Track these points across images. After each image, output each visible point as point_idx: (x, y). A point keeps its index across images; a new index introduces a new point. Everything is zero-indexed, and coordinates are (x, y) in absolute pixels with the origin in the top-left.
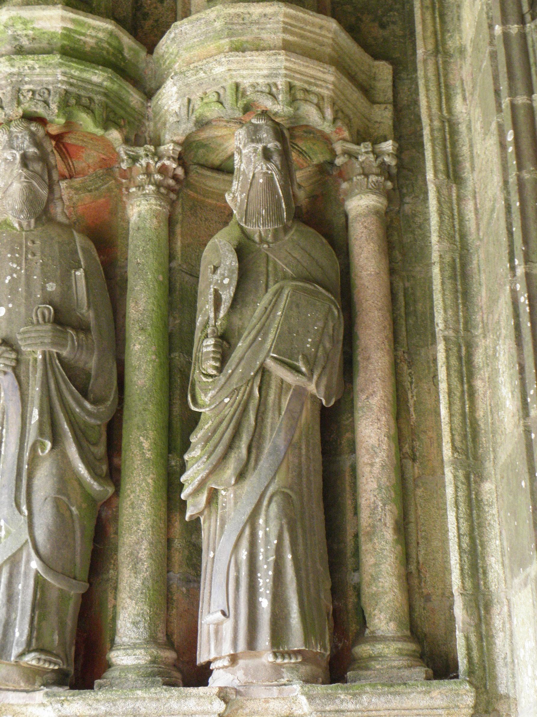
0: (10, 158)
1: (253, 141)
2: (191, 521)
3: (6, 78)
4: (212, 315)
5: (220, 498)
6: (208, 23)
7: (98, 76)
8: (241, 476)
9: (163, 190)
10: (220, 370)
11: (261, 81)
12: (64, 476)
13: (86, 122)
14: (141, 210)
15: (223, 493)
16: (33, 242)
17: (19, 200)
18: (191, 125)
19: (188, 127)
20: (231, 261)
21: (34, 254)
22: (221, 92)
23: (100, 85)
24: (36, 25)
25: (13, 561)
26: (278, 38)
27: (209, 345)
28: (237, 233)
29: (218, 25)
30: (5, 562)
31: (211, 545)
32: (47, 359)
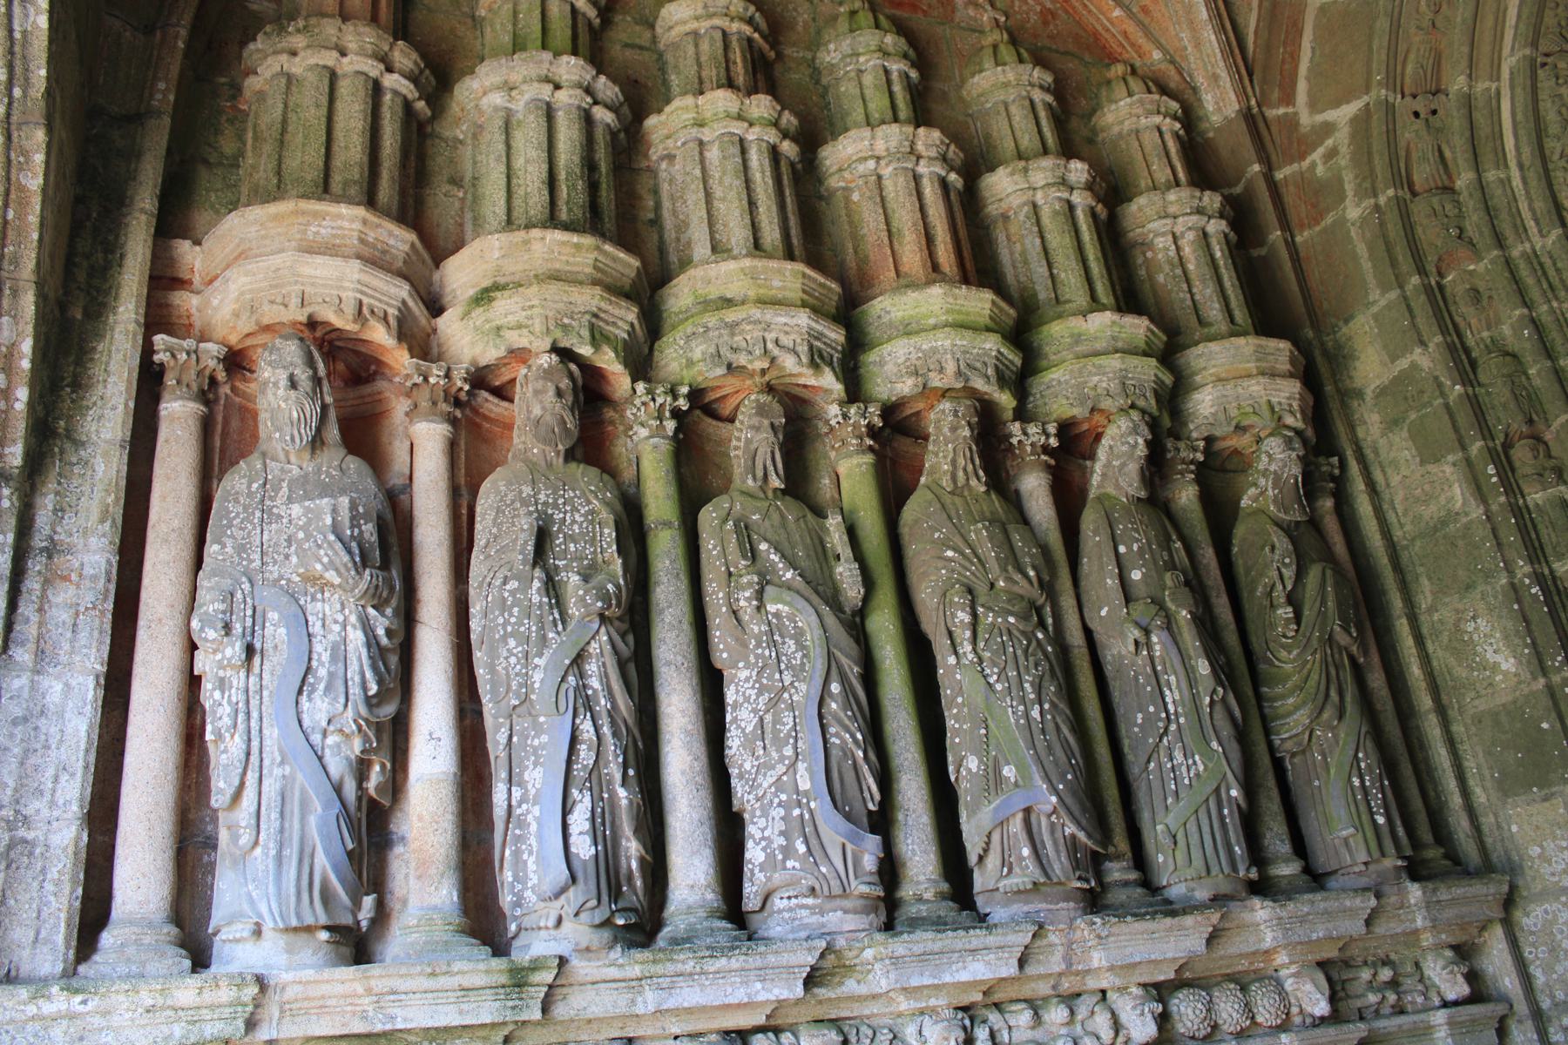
6: (1237, 348)
8: (1340, 718)
25: (1217, 790)
27: (1285, 612)
31: (1312, 774)
32: (1195, 617)
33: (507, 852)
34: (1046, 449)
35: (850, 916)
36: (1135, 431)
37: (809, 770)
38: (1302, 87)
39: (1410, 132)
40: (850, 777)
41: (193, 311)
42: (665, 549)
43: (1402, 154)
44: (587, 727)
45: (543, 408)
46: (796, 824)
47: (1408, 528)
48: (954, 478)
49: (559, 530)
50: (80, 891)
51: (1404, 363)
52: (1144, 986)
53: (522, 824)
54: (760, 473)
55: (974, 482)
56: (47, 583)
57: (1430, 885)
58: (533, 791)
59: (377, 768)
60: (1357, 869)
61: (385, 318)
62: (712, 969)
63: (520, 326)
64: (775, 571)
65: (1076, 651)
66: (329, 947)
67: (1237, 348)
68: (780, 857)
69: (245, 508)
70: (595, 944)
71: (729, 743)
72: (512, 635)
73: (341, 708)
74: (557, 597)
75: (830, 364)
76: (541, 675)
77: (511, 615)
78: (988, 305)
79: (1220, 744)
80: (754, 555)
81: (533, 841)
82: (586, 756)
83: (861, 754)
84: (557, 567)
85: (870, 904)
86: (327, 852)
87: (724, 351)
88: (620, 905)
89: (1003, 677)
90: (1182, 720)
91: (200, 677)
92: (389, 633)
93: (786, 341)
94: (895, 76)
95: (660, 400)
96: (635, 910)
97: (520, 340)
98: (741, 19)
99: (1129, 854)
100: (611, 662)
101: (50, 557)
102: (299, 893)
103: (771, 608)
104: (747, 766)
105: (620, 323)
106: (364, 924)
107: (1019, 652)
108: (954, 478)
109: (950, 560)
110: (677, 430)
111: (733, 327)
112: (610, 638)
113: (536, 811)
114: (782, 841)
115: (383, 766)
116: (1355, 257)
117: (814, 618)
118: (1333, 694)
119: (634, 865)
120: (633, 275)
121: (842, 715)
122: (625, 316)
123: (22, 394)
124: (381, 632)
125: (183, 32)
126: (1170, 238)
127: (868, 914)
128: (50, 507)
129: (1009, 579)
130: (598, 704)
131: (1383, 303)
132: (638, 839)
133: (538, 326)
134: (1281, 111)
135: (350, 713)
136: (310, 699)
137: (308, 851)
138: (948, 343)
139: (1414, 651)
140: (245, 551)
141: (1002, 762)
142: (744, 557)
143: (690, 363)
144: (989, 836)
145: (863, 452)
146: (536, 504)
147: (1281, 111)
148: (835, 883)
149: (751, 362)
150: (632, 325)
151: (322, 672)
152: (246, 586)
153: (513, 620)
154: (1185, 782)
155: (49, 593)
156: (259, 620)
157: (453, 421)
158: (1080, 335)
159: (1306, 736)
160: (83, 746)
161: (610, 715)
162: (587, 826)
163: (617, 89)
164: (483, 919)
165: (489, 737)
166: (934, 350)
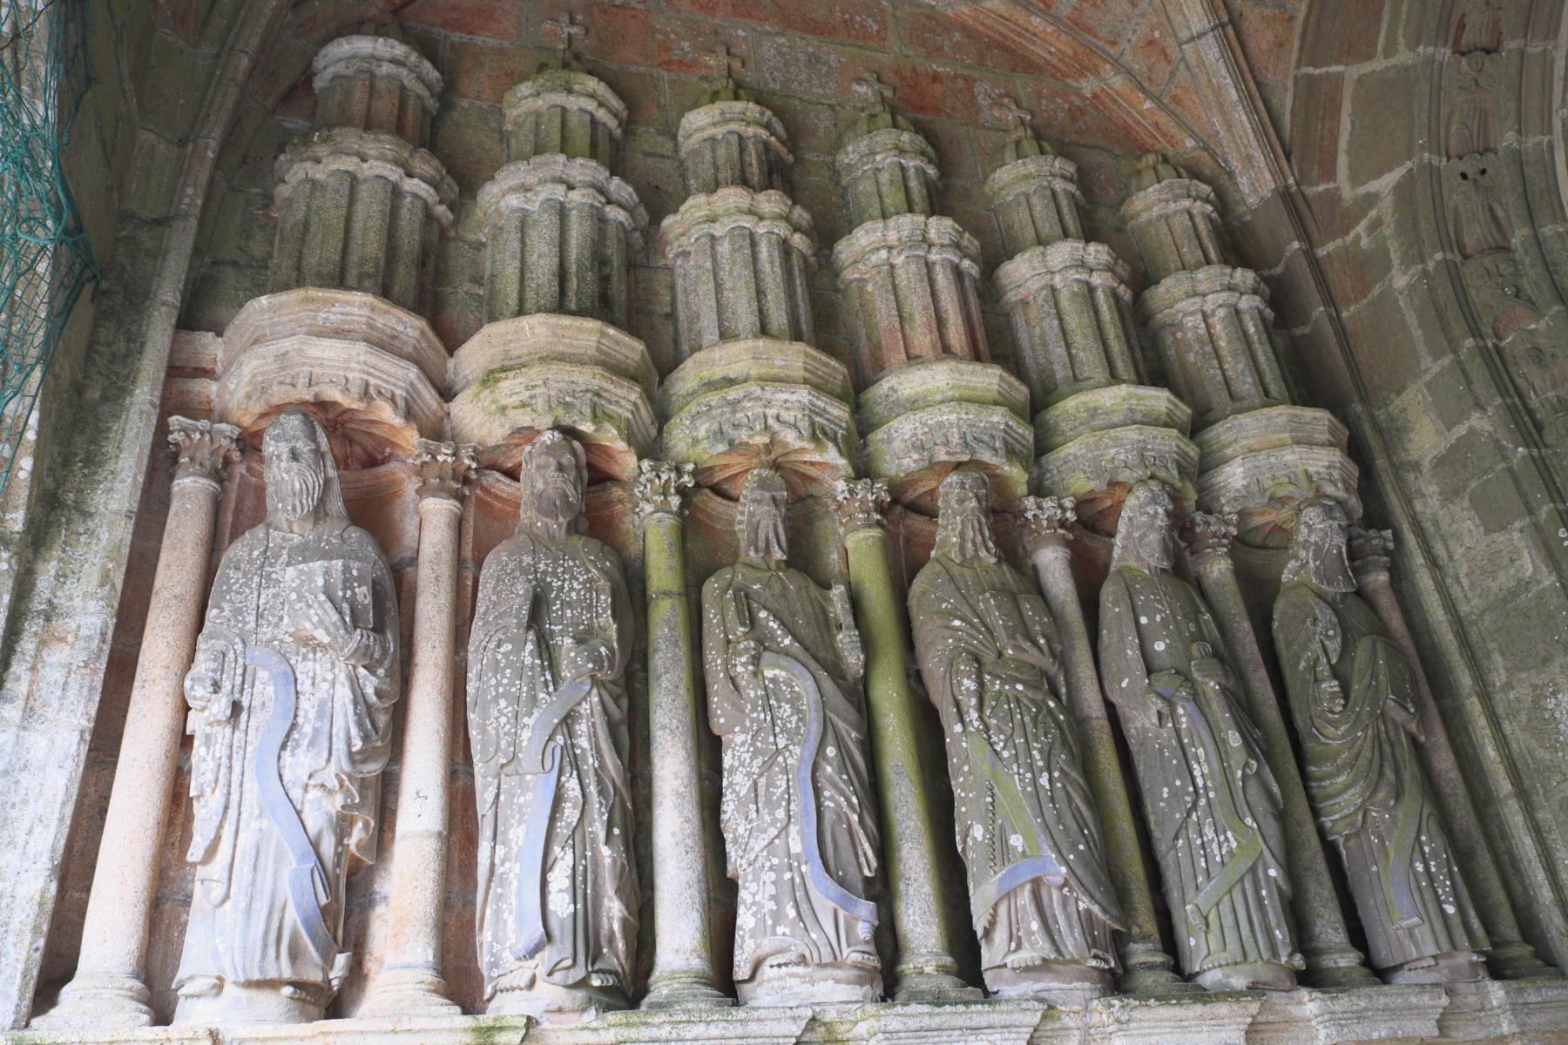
6: (1269, 419)
8: (1398, 798)
10: (1344, 706)
25: (1253, 870)
26: (1325, 437)
27: (1330, 686)
29: (1281, 420)
32: (1224, 689)
33: (488, 911)
34: (1063, 524)
35: (842, 986)
36: (1154, 500)
37: (800, 832)
38: (1342, 162)
39: (1457, 196)
40: (844, 841)
41: (213, 397)
42: (665, 618)
43: (1450, 216)
44: (572, 785)
45: (546, 483)
46: (787, 889)
47: (1475, 602)
48: (962, 548)
49: (557, 597)
50: (41, 942)
51: (1461, 430)
53: (504, 882)
54: (762, 545)
55: (983, 553)
56: (43, 643)
57: (1514, 984)
58: (515, 849)
59: (360, 825)
60: (1425, 963)
61: (393, 400)
62: (689, 1036)
63: (523, 405)
64: (773, 638)
65: (1095, 723)
66: (293, 1004)
67: (1269, 419)
68: (770, 922)
69: (245, 574)
70: (568, 1005)
71: (724, 807)
72: (504, 695)
73: (323, 762)
74: (550, 659)
75: (835, 440)
76: (531, 733)
77: (503, 677)
78: (996, 381)
79: (1255, 820)
80: (753, 622)
81: (513, 900)
82: (570, 813)
83: (855, 818)
84: (552, 632)
85: (863, 976)
86: (298, 906)
87: (726, 428)
88: (596, 967)
89: (1010, 744)
90: (1212, 795)
91: (192, 737)
92: (378, 693)
93: (787, 416)
94: (912, 172)
95: (664, 477)
96: (616, 973)
97: (524, 419)
98: (758, 123)
99: (1156, 936)
101: (48, 619)
102: (265, 946)
103: (769, 673)
104: (741, 830)
105: (623, 402)
106: (335, 983)
107: (1027, 719)
108: (962, 548)
109: (957, 629)
110: (683, 506)
111: (734, 405)
112: (602, 701)
113: (517, 868)
114: (772, 905)
115: (366, 825)
116: (1405, 328)
118: (1389, 774)
119: (616, 926)
120: (637, 358)
121: (837, 778)
122: (627, 399)
123: (26, 463)
124: (370, 691)
125: (213, 143)
126: (1200, 316)
127: (862, 985)
128: (52, 572)
129: (1015, 647)
130: (586, 763)
131: (1435, 369)
132: (621, 899)
133: (540, 404)
134: (1322, 188)
135: (332, 768)
136: (293, 754)
137: (279, 905)
138: (953, 417)
139: (1487, 731)
140: (241, 613)
141: (1009, 831)
142: (743, 624)
143: (696, 441)
144: (995, 907)
145: (870, 526)
146: (536, 572)
147: (1322, 188)
148: (825, 951)
149: (751, 437)
150: (635, 404)
151: (308, 729)
152: (239, 647)
153: (505, 681)
154: (1219, 862)
155: (44, 653)
156: (249, 679)
157: (461, 499)
158: (1096, 409)
159: (1360, 818)
160: (60, 798)
161: (597, 774)
162: (567, 883)
163: (630, 189)
164: (459, 980)
165: (478, 796)
166: (940, 425)
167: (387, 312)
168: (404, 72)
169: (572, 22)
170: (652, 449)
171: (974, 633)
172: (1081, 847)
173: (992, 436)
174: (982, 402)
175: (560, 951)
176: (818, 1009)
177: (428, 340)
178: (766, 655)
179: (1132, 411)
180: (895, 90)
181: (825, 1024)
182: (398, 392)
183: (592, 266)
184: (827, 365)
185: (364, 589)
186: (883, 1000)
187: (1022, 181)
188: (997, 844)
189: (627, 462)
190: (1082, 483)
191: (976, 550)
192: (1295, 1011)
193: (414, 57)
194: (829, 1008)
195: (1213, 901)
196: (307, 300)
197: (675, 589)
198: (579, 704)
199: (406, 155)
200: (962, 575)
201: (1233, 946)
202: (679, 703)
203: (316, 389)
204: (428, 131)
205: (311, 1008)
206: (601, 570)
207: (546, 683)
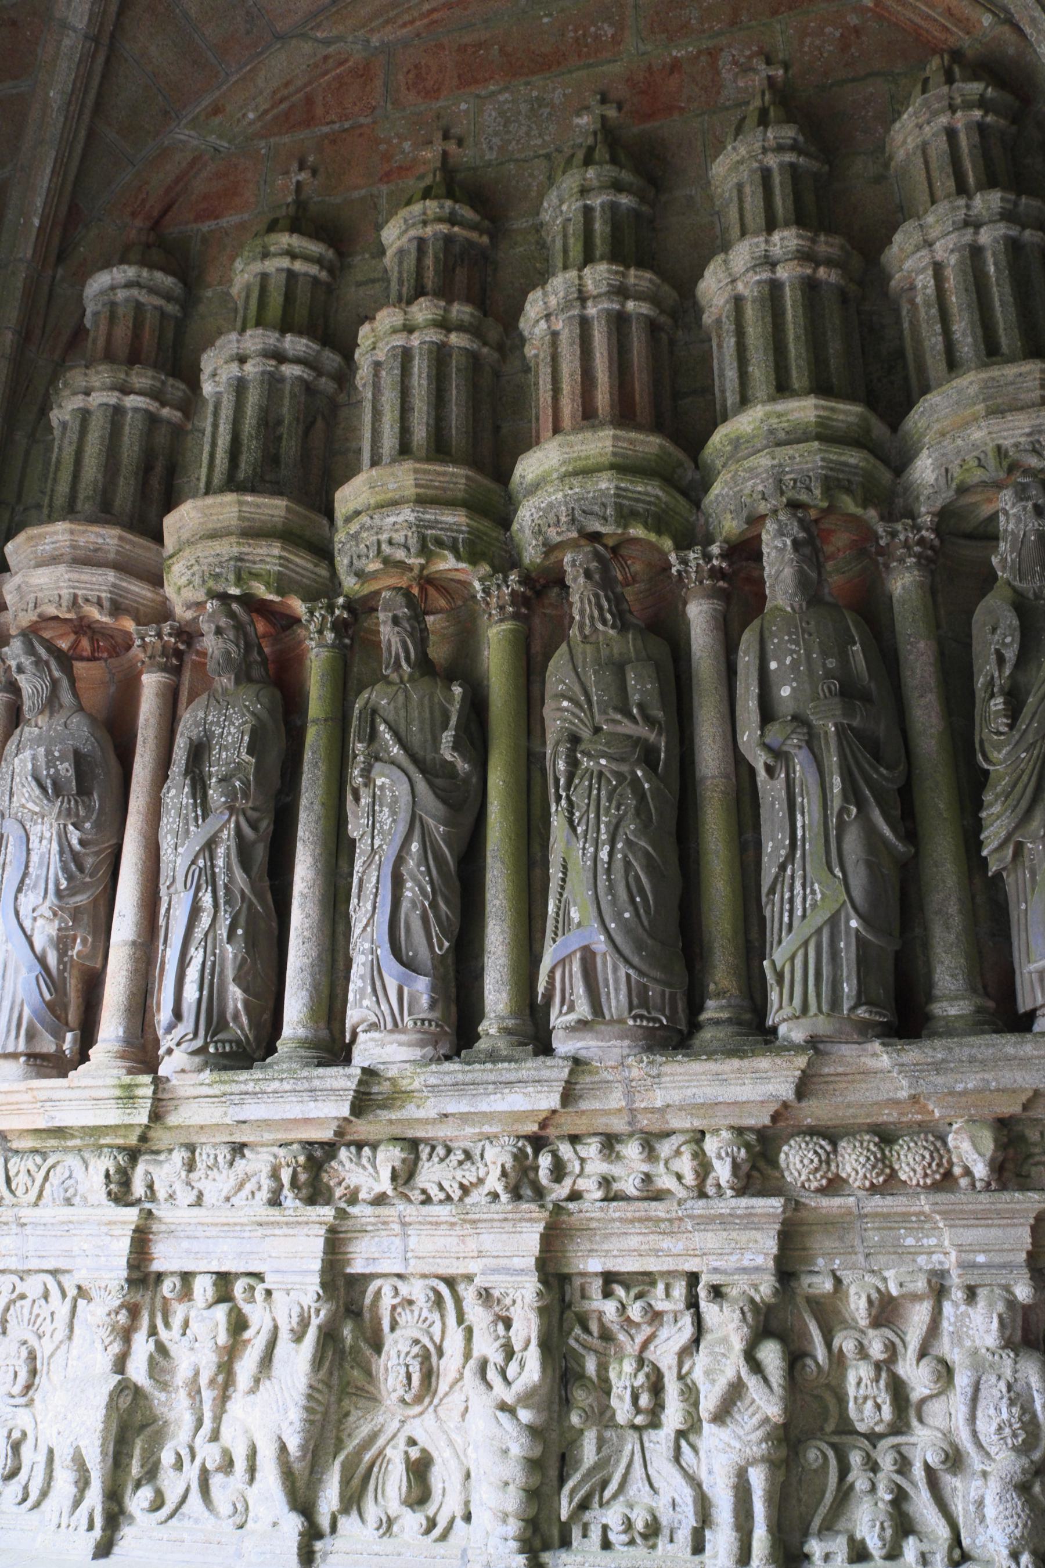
0: (780, 545)
1: (1022, 500)
2: (993, 877)
3: (767, 471)
4: (996, 674)
5: (1026, 851)
6: (959, 392)
7: (853, 457)
9: (923, 561)
10: (1011, 727)
11: (1022, 440)
12: (871, 838)
13: (849, 504)
14: (903, 583)
15: (1030, 845)
16: (808, 623)
17: (791, 584)
18: (952, 493)
19: (947, 495)
20: (1010, 619)
21: (810, 635)
22: (982, 456)
23: (856, 467)
24: (790, 417)
25: (833, 922)
27: (998, 703)
28: (1008, 593)
29: (972, 390)
30: (825, 923)
31: (1021, 897)
32: (841, 731)
34: (716, 574)
35: (404, 1048)
36: (780, 533)
46: (369, 969)
48: (582, 626)
52: (739, 1131)
55: (600, 627)
61: (99, 603)
63: (190, 582)
65: (709, 782)
66: (30, 1069)
67: (959, 392)
70: (187, 1068)
76: (181, 863)
78: (609, 443)
80: (373, 736)
82: (205, 920)
83: (426, 904)
89: (584, 821)
92: (81, 842)
93: (399, 537)
96: (239, 1042)
98: (439, 220)
100: (232, 844)
102: (8, 1031)
103: (379, 782)
105: (268, 559)
108: (582, 626)
109: (566, 710)
115: (84, 941)
117: (406, 787)
119: (240, 1006)
120: (283, 514)
122: (269, 555)
124: (74, 842)
126: (930, 272)
127: (423, 1047)
129: (607, 721)
132: (239, 986)
133: (197, 580)
135: (48, 903)
138: (560, 495)
142: (360, 741)
145: (501, 621)
148: (389, 1019)
150: (281, 557)
158: (738, 438)
159: (1011, 851)
161: (226, 886)
163: (304, 341)
166: (551, 505)
167: (84, 532)
168: (135, 292)
169: (301, 168)
170: (323, 591)
171: (577, 711)
172: (627, 915)
173: (604, 505)
174: (586, 472)
175: (186, 1027)
176: (382, 1067)
177: (130, 542)
178: (378, 766)
179: (772, 432)
180: (620, 108)
181: (389, 1079)
182: (103, 595)
183: (258, 432)
184: (444, 474)
185: (66, 765)
186: (448, 1058)
187: (735, 167)
188: (560, 919)
189: (299, 606)
190: (730, 525)
191: (593, 625)
192: (871, 1063)
193: (145, 273)
194: (390, 1066)
195: (788, 955)
196: (30, 538)
197: (322, 716)
198: (221, 830)
199: (123, 376)
200: (584, 653)
201: (797, 1001)
202: (313, 817)
203: (38, 610)
204: (170, 335)
205: (48, 1071)
206: (253, 714)
207: (196, 819)
